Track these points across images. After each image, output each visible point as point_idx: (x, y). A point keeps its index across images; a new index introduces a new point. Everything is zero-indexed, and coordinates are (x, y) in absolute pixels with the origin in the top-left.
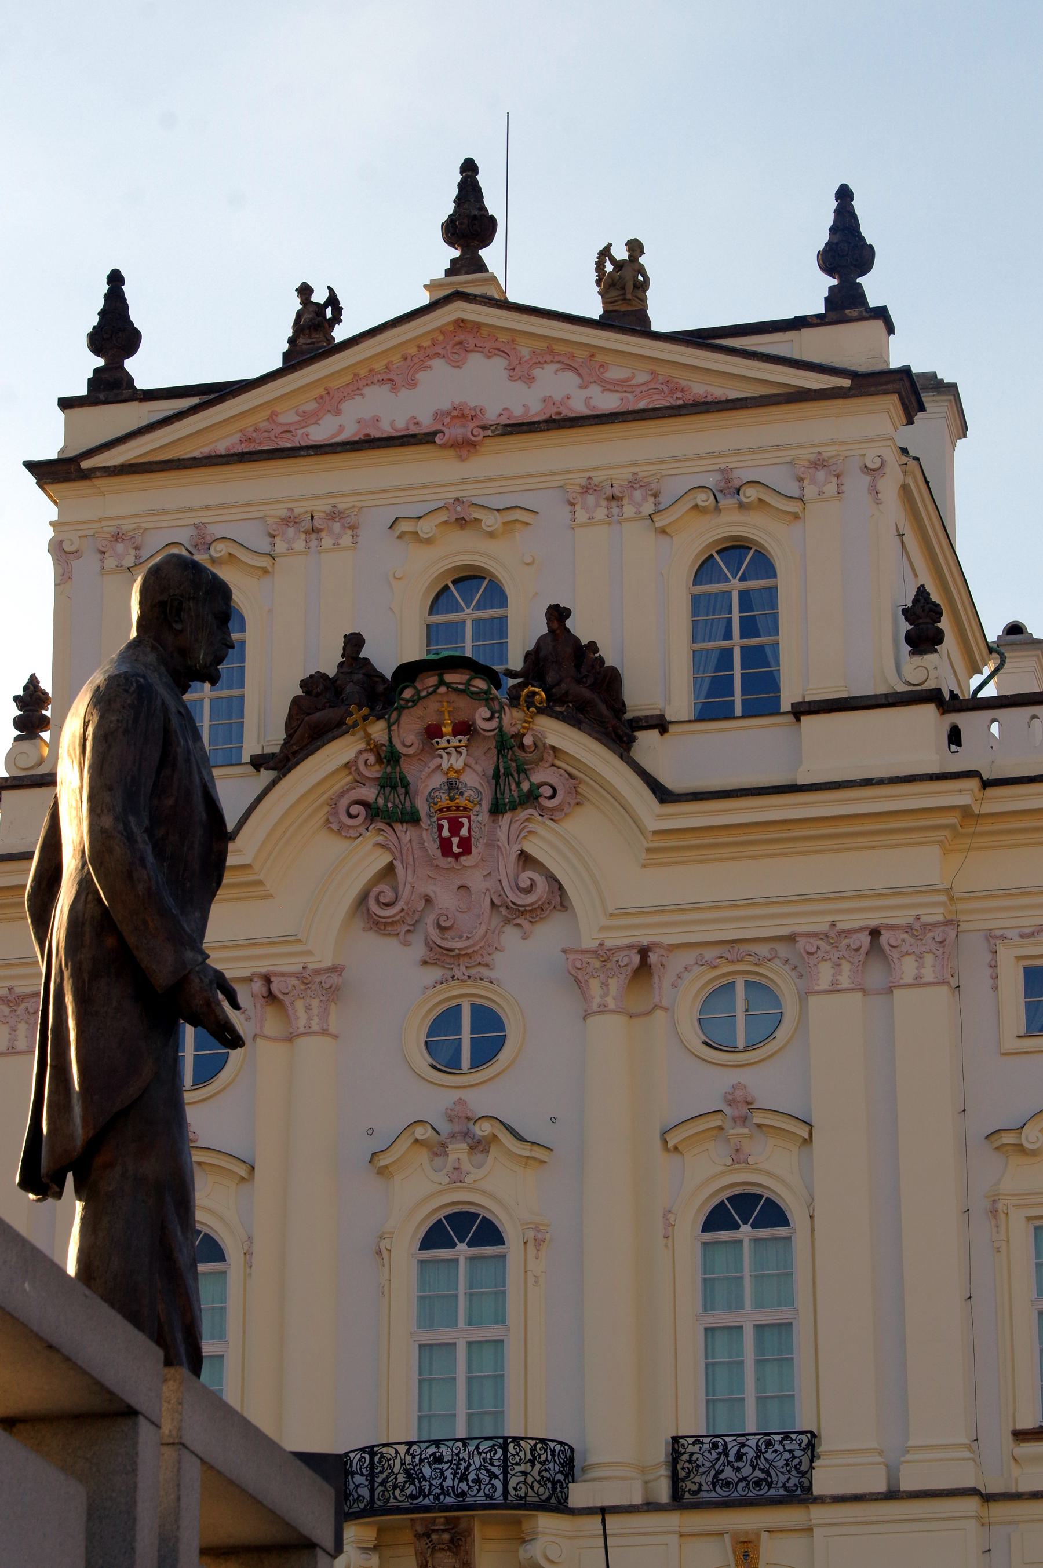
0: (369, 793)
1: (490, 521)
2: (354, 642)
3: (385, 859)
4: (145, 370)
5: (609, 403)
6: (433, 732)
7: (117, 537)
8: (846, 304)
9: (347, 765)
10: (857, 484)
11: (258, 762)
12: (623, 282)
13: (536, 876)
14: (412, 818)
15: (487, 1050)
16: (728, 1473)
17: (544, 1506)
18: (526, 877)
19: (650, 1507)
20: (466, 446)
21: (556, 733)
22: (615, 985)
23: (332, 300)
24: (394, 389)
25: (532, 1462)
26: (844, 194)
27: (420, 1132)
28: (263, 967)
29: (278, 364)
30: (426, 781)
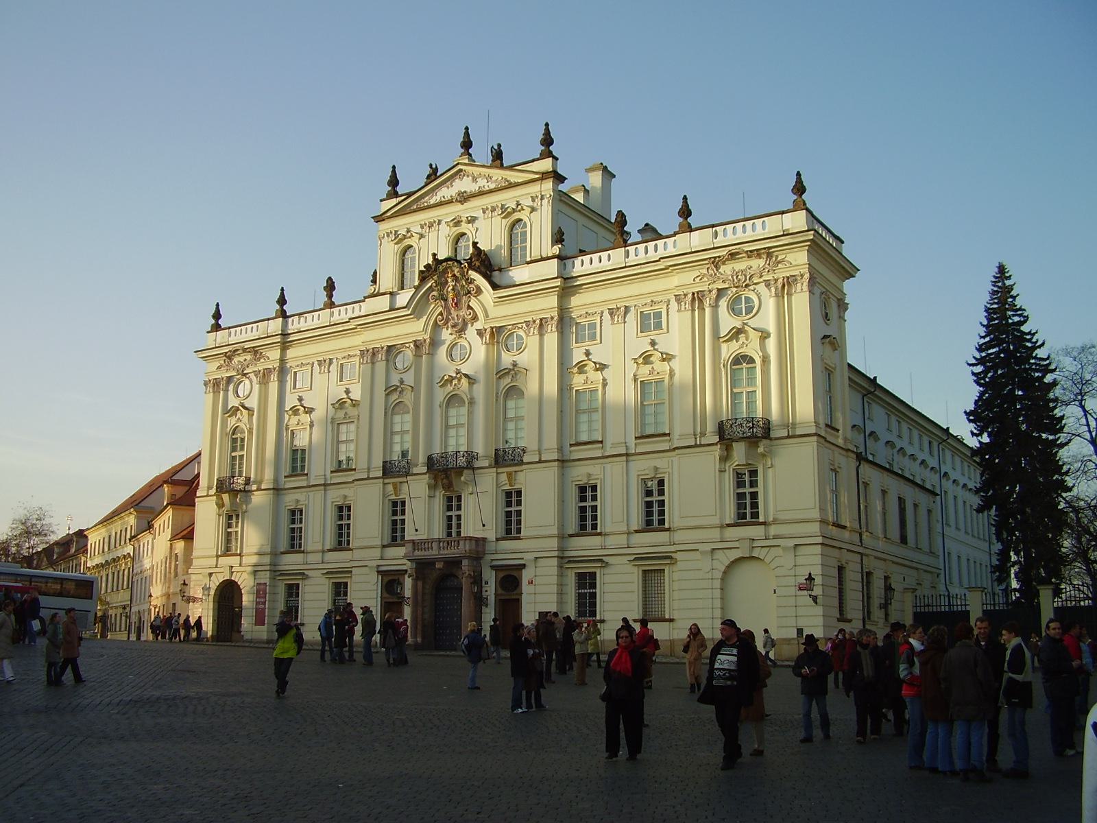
2: (434, 255)
3: (440, 309)
4: (400, 190)
5: (492, 186)
9: (431, 287)
11: (414, 287)
12: (498, 156)
13: (471, 311)
16: (506, 458)
17: (467, 468)
19: (490, 467)
21: (473, 275)
24: (448, 188)
25: (463, 457)
27: (446, 378)
29: (424, 184)
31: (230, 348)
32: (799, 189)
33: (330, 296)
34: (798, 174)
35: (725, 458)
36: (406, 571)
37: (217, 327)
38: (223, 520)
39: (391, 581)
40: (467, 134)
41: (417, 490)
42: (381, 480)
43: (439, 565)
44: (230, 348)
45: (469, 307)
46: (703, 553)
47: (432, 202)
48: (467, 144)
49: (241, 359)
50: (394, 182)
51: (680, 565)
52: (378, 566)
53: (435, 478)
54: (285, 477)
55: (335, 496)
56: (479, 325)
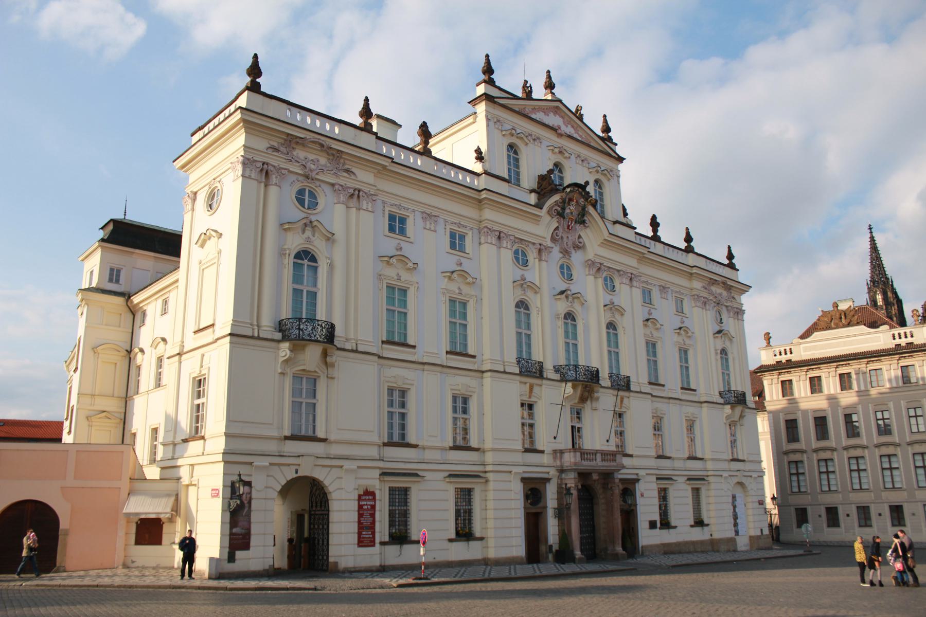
0: (559, 209)
1: (567, 155)
2: (551, 172)
6: (571, 200)
7: (498, 121)
8: (610, 139)
10: (616, 178)
11: (532, 191)
14: (564, 218)
15: (570, 277)
18: (581, 240)
20: (560, 135)
21: (591, 209)
22: (595, 270)
23: (530, 86)
26: (605, 116)
28: (541, 242)
30: (567, 211)
31: (309, 136)
32: (730, 256)
33: (426, 142)
34: (729, 247)
35: (728, 417)
36: (548, 480)
37: (254, 87)
38: (288, 382)
39: (533, 492)
40: (549, 77)
41: (553, 397)
42: (518, 378)
43: (595, 477)
44: (309, 136)
45: (580, 237)
46: (726, 478)
47: (533, 116)
48: (550, 86)
49: (311, 157)
50: (488, 70)
51: (713, 486)
52: (524, 472)
53: (574, 387)
54: (383, 342)
55: (461, 382)
56: (590, 256)
